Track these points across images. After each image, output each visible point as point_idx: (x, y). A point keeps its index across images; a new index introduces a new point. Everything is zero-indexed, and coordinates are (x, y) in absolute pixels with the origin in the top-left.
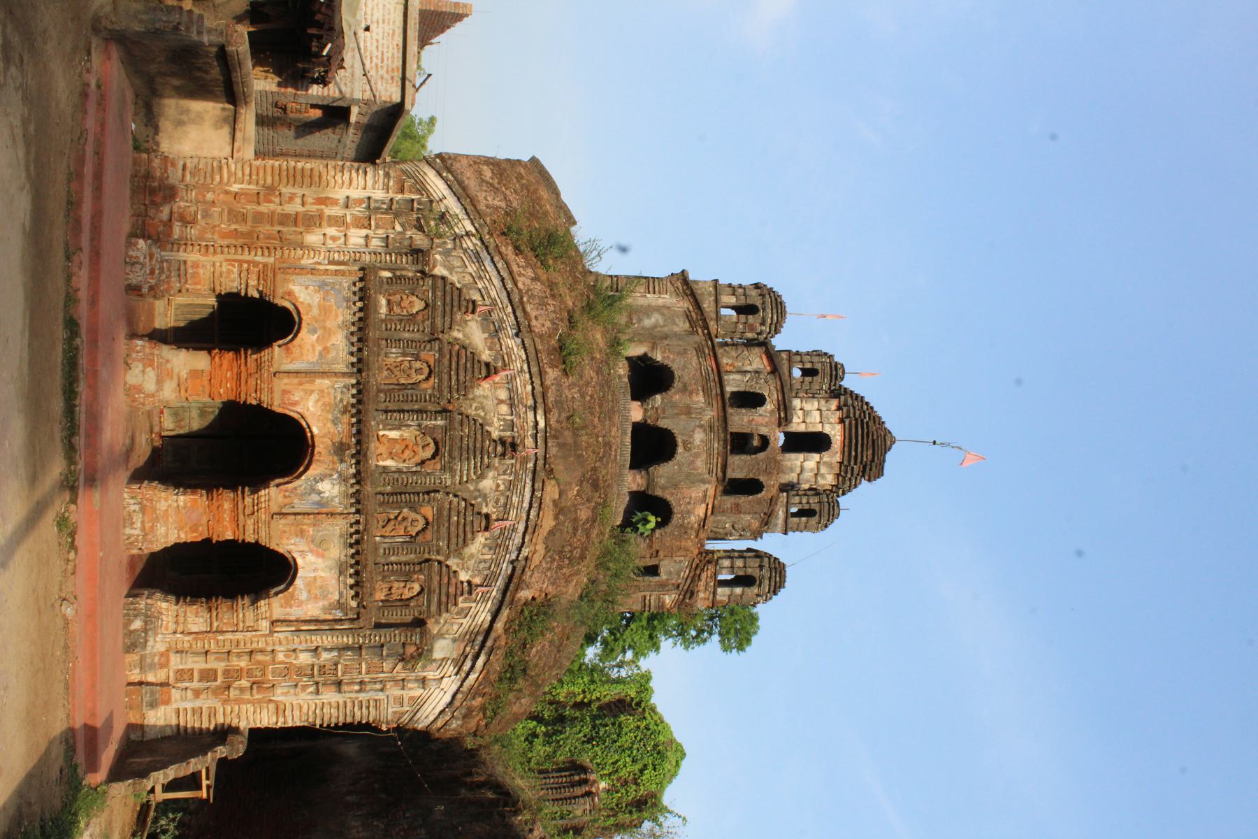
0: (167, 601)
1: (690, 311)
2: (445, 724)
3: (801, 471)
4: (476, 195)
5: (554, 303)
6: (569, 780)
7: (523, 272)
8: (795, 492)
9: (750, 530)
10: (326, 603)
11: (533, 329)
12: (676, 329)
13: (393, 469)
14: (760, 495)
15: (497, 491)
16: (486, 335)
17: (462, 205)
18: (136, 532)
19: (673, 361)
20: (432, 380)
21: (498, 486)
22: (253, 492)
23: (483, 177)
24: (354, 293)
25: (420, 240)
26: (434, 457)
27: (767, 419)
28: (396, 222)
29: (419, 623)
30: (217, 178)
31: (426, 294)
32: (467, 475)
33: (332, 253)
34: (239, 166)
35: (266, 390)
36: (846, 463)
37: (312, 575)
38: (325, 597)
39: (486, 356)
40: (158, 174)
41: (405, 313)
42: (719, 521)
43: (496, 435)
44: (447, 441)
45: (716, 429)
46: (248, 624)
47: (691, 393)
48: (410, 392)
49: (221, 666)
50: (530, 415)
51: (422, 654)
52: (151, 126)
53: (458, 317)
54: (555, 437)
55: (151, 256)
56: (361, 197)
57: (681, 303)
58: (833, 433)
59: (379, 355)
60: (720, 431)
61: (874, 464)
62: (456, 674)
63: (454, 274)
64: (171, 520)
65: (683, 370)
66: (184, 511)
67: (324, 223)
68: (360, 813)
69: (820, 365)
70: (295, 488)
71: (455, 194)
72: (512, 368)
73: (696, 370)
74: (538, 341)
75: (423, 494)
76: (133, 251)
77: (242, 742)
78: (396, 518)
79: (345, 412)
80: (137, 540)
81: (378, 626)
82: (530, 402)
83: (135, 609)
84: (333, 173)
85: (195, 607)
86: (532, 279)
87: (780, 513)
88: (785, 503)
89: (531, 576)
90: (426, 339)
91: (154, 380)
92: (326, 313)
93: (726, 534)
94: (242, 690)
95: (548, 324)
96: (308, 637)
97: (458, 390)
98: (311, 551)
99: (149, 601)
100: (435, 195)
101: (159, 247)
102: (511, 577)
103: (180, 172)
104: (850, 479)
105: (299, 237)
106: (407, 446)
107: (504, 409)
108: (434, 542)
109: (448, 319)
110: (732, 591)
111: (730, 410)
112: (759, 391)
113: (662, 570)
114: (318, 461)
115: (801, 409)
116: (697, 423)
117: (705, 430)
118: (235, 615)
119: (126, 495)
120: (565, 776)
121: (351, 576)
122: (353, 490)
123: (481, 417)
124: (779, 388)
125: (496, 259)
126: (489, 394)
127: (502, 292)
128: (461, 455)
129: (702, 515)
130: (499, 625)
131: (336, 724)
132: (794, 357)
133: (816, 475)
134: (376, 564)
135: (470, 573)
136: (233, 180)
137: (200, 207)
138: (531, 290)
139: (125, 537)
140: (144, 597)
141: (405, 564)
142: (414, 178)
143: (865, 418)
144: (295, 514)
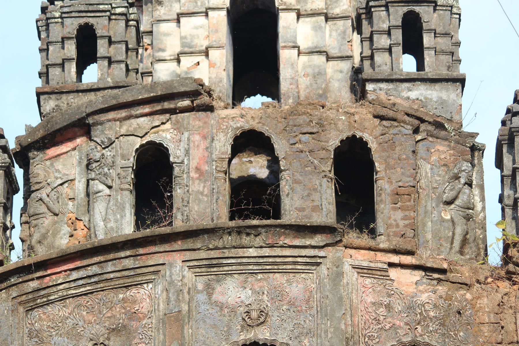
3: (320, 52)
8: (367, 64)
9: (455, 163)
14: (373, 145)
27: (197, 138)
42: (436, 235)
47: (133, 316)
88: (391, 86)
93: (468, 218)
112: (132, 159)
115: (179, 61)
116: (202, 297)
117: (220, 278)
124: (123, 113)
129: (418, 275)
132: (53, 83)
133: (327, 19)
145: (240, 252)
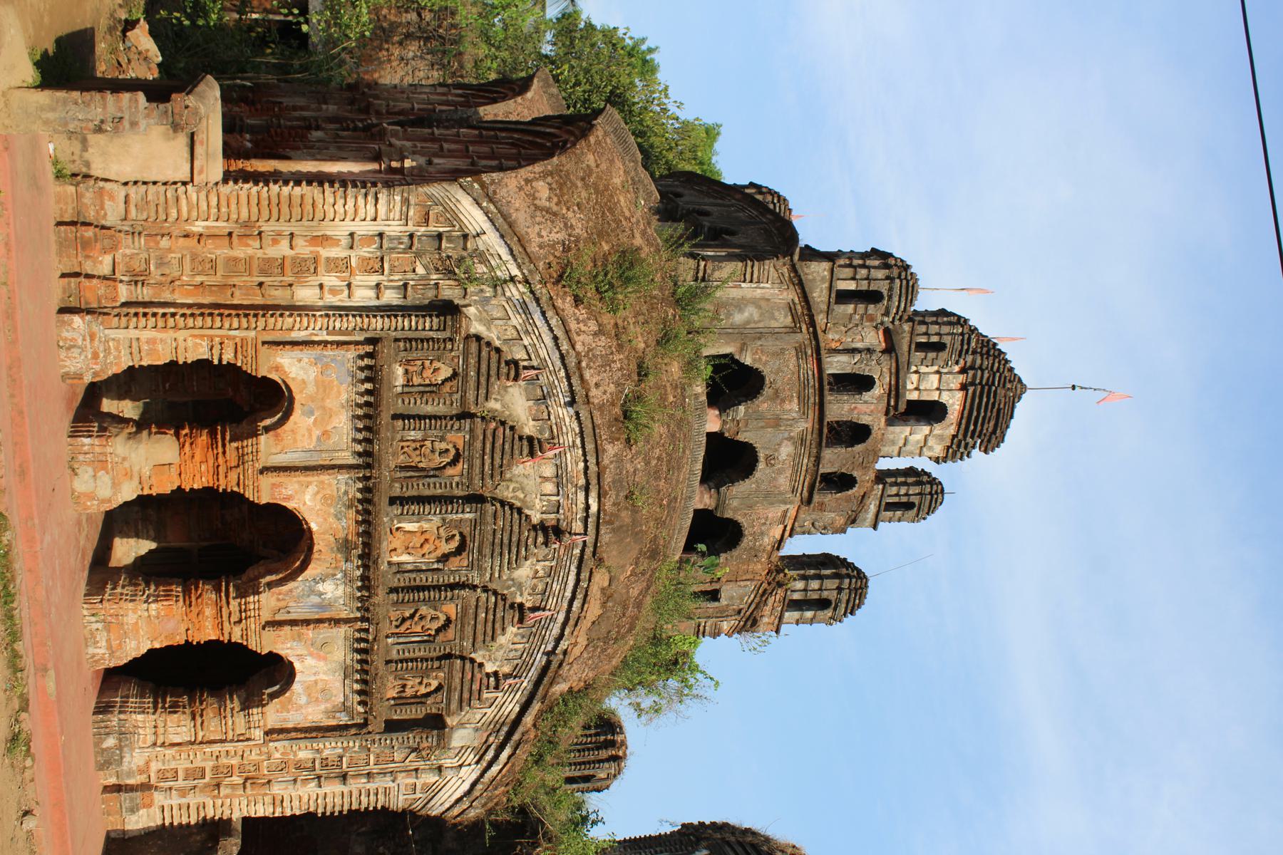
0: (143, 712)
1: (794, 304)
2: (462, 813)
3: (905, 444)
4: (527, 233)
5: (622, 356)
6: (594, 739)
7: (583, 328)
10: (329, 705)
11: (591, 400)
12: (774, 324)
13: (409, 567)
14: (850, 492)
15: (534, 578)
16: (531, 403)
17: (506, 243)
18: (101, 651)
19: (765, 364)
20: (460, 466)
21: (537, 572)
22: (242, 594)
23: (537, 202)
24: (361, 369)
25: (449, 291)
26: (460, 550)
27: (872, 407)
28: (418, 263)
29: (435, 723)
30: (174, 214)
31: (456, 360)
32: (500, 571)
33: (332, 319)
34: (203, 195)
35: (251, 487)
36: (960, 437)
37: (313, 678)
38: (327, 701)
39: (529, 428)
40: (92, 213)
41: (427, 382)
43: (536, 518)
44: (477, 536)
45: (808, 442)
46: (238, 732)
47: (783, 401)
48: (432, 480)
49: (209, 765)
50: (581, 496)
51: (443, 743)
52: (76, 139)
53: (496, 387)
54: (610, 522)
55: (92, 337)
56: (371, 233)
57: (785, 293)
58: (951, 401)
59: (393, 439)
60: (813, 446)
61: (994, 436)
62: (477, 763)
63: (493, 329)
64: (142, 633)
65: (777, 373)
66: (157, 621)
67: (321, 269)
68: (364, 829)
69: (950, 337)
70: (291, 591)
71: (498, 230)
72: (561, 441)
73: (793, 373)
74: (596, 414)
75: (446, 591)
76: (68, 331)
77: (236, 844)
78: (412, 616)
79: (350, 507)
80: (103, 659)
81: (392, 726)
82: (582, 482)
83: (106, 727)
84: (332, 201)
85: (175, 716)
86: (595, 334)
87: (872, 507)
89: (569, 670)
90: (454, 412)
91: (109, 483)
92: (325, 391)
94: (233, 786)
95: (612, 388)
96: (309, 745)
97: (492, 476)
98: (311, 654)
99: (122, 716)
100: (470, 228)
101: (102, 323)
102: (545, 670)
103: (122, 206)
104: (962, 453)
105: (288, 292)
106: (426, 540)
107: (549, 487)
108: (457, 641)
109: (482, 391)
110: (802, 615)
111: (829, 397)
113: (723, 595)
114: (317, 559)
116: (786, 435)
117: (794, 443)
118: (223, 722)
119: (85, 612)
120: (591, 735)
121: (357, 681)
122: (359, 594)
123: (520, 500)
124: (893, 371)
125: (550, 314)
126: (532, 471)
127: (554, 353)
128: (493, 551)
129: (778, 537)
130: (528, 719)
131: (341, 812)
134: (388, 662)
135: (498, 663)
136: (195, 214)
137: (152, 255)
138: (591, 350)
139: (88, 656)
140: (117, 709)
141: (422, 661)
142: (442, 205)
143: (993, 383)
144: (293, 623)
145: (806, 456)
